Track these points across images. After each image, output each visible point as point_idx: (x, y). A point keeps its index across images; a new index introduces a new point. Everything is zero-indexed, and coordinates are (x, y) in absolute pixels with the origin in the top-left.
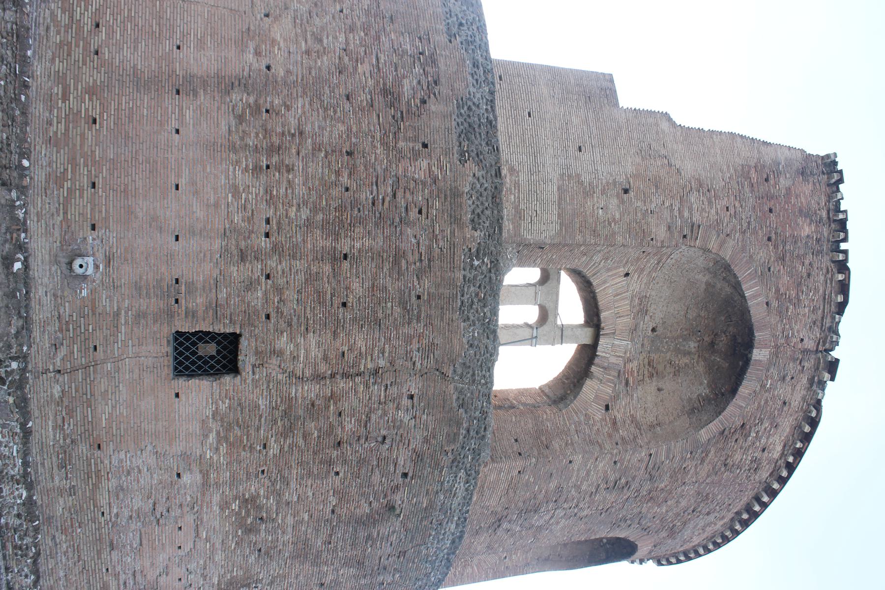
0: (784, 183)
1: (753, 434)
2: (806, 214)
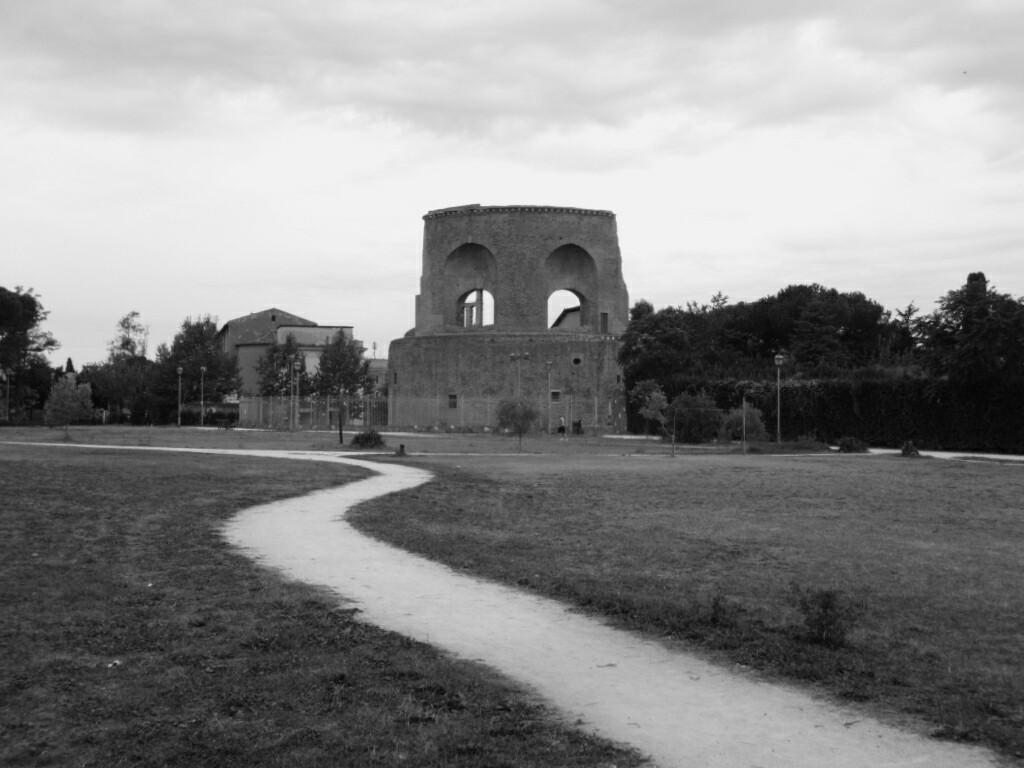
0: (430, 237)
1: (499, 230)
2: (436, 227)
